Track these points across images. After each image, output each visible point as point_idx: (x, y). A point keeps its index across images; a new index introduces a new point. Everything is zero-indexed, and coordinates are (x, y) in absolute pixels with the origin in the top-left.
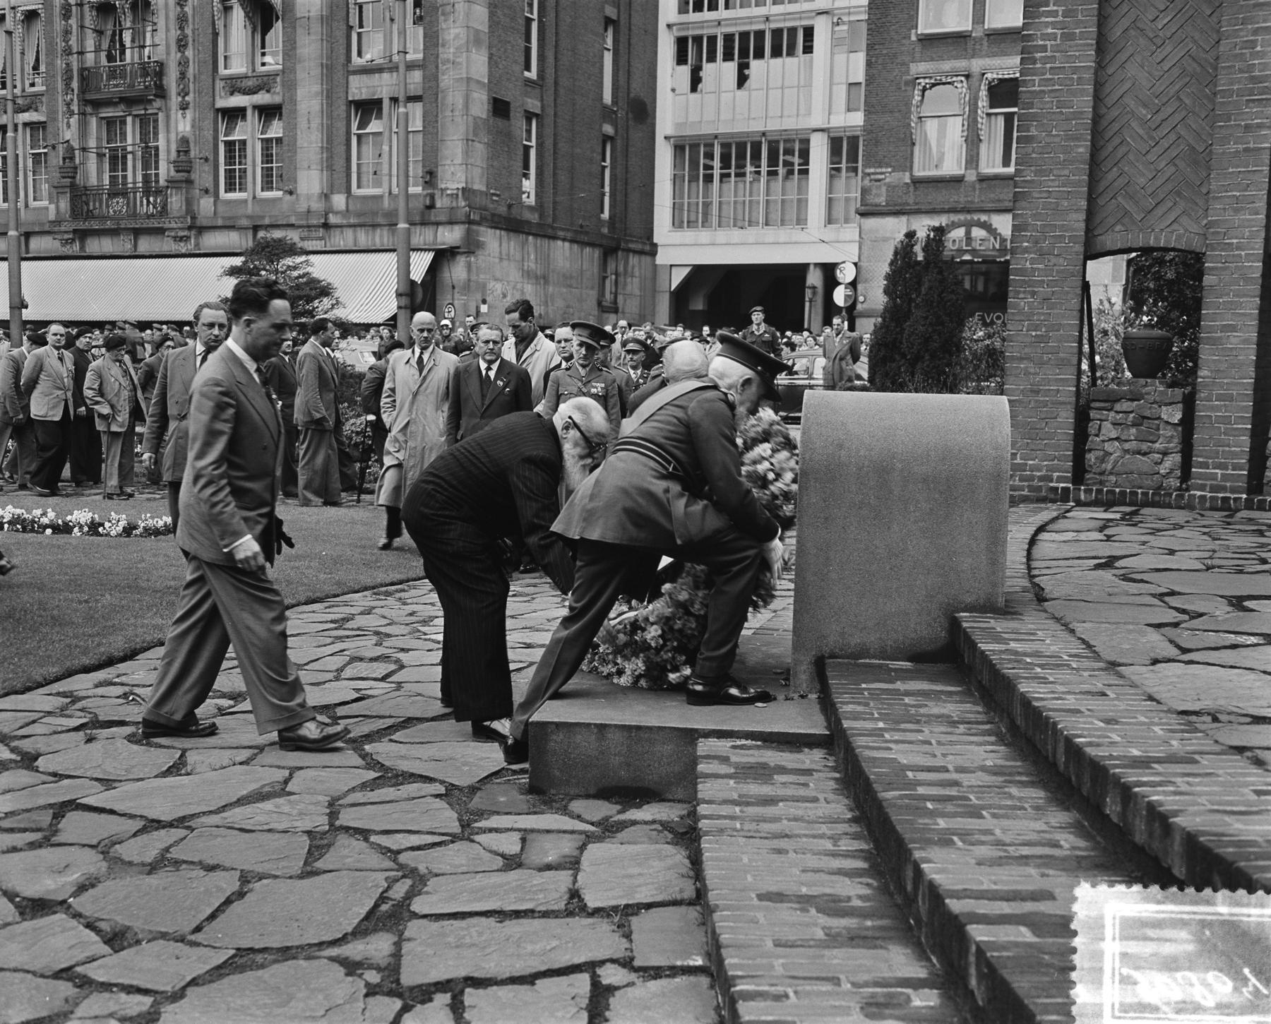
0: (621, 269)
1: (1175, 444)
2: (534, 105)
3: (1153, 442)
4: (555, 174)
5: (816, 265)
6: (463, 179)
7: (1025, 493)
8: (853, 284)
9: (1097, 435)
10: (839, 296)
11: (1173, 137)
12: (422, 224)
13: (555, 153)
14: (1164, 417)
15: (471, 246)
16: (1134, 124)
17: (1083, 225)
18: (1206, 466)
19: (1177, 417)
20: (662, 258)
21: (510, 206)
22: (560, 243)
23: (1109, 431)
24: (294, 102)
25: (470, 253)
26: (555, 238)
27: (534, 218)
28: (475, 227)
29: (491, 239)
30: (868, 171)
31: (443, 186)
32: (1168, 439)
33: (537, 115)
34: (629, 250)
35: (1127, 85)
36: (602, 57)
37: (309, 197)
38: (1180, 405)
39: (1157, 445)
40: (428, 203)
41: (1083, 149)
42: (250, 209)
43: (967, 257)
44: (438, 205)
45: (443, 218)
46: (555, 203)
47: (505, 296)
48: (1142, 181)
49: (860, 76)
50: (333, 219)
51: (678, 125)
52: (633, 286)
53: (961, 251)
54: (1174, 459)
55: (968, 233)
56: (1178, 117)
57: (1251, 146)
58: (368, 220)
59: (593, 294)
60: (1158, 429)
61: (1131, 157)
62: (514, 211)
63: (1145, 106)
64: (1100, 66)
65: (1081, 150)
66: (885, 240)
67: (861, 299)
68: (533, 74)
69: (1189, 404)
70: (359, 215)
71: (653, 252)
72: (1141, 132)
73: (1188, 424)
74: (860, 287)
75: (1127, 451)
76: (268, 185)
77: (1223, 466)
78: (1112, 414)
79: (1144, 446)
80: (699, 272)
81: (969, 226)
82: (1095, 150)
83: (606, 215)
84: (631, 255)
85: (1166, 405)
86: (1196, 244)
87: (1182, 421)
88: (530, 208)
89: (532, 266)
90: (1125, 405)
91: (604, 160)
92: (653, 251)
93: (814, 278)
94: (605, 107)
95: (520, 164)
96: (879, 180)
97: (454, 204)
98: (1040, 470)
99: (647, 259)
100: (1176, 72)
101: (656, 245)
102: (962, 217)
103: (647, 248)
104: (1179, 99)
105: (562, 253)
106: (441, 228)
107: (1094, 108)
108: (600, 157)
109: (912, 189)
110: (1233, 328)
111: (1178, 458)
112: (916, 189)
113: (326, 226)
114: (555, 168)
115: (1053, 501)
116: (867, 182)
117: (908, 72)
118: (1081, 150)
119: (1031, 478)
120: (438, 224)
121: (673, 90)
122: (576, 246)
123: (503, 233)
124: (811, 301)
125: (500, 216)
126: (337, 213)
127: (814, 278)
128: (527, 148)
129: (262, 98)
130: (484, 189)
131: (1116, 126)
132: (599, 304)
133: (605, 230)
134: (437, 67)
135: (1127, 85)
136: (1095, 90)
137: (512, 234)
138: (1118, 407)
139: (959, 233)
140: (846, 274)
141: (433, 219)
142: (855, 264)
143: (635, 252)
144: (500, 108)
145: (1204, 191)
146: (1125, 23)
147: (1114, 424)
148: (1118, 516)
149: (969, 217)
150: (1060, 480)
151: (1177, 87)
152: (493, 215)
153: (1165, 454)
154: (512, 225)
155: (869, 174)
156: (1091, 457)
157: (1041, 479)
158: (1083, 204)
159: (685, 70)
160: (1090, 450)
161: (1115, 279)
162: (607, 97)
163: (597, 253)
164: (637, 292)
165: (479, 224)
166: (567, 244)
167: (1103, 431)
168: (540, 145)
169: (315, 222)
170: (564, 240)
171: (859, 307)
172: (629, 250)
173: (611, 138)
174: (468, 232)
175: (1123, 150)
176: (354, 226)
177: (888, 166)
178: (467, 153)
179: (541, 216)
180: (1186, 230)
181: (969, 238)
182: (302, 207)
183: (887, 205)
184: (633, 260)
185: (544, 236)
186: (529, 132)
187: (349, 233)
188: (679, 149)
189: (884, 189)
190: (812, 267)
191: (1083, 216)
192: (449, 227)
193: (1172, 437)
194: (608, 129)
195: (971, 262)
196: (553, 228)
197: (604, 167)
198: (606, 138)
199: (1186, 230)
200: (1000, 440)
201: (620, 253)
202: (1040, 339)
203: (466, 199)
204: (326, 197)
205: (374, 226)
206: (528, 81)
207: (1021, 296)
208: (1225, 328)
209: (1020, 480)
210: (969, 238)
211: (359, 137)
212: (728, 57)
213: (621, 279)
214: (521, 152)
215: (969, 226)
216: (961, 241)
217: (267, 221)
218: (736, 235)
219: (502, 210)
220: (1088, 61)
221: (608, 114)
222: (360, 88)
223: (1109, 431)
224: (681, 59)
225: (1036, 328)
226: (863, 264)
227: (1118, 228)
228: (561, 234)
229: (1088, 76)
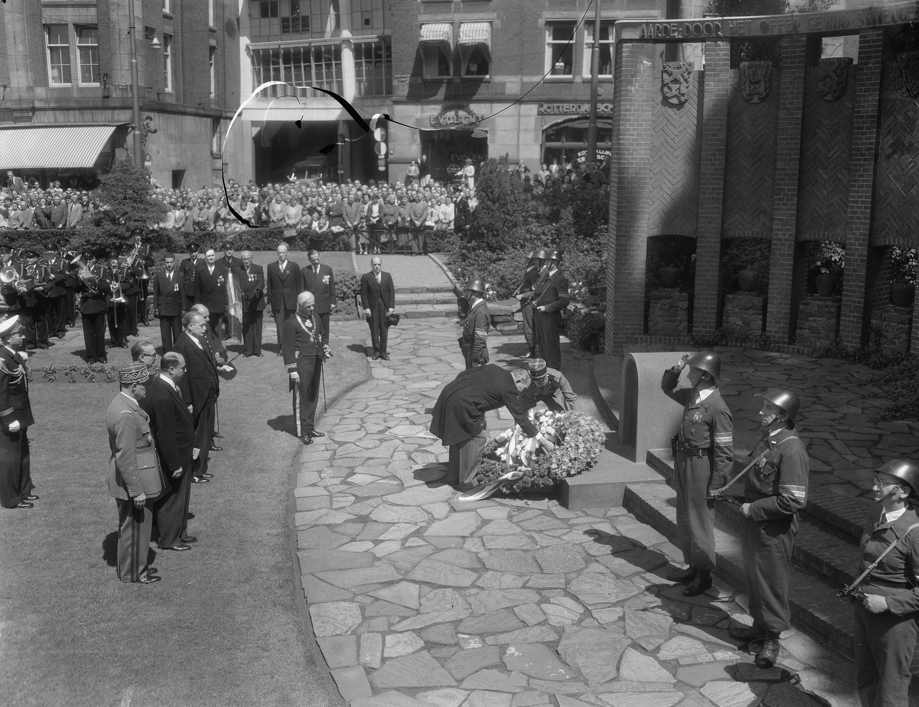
1: (685, 317)
18: (698, 327)
19: (686, 306)
32: (682, 316)
37: (19, 89)
45: (117, 104)
47: (158, 153)
54: (684, 324)
58: (64, 105)
67: (392, 152)
73: (690, 309)
77: (706, 327)
89: (173, 132)
134: (108, 7)
150: (640, 334)
156: (651, 324)
161: (536, 141)
171: (390, 157)
176: (54, 109)
182: (15, 96)
187: (50, 114)
204: (30, 89)
218: (293, 104)
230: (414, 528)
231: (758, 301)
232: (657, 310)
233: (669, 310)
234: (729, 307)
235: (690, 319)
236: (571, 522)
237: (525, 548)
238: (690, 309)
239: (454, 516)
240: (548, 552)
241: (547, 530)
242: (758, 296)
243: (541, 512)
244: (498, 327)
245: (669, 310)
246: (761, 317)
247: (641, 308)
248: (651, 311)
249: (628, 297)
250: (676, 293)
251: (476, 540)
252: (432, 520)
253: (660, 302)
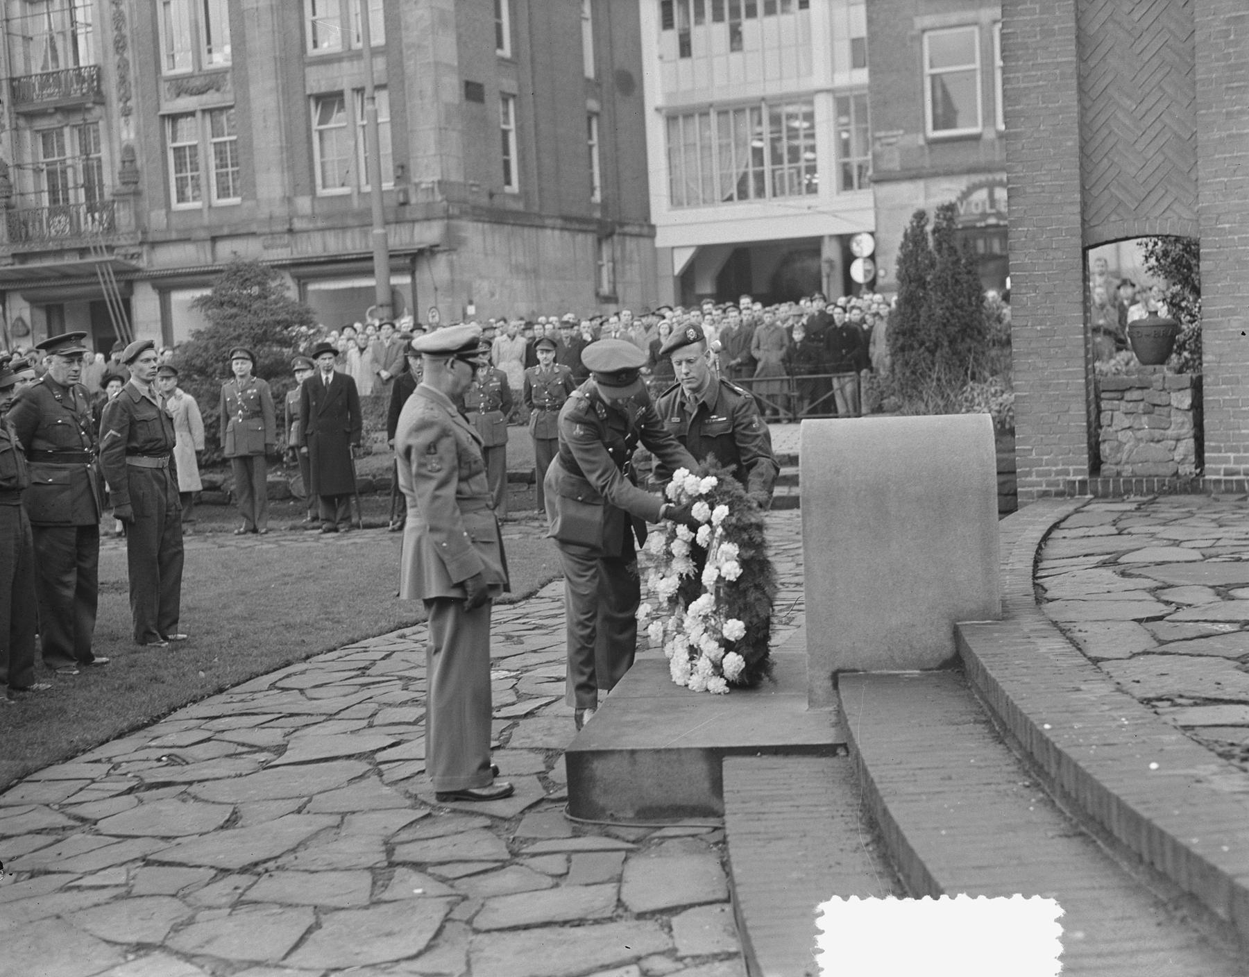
0: (618, 254)
2: (510, 85)
3: (1165, 429)
4: (538, 159)
5: (831, 236)
6: (438, 171)
7: (1044, 488)
8: (872, 257)
10: (858, 272)
11: (1158, 126)
12: (397, 223)
13: (536, 134)
15: (452, 243)
16: (1120, 115)
17: (1078, 218)
19: (1187, 402)
20: (660, 242)
21: (491, 195)
22: (549, 232)
23: (1121, 421)
24: (247, 100)
25: (451, 250)
26: (543, 227)
27: (519, 206)
28: (454, 222)
29: (474, 234)
30: (878, 134)
31: (417, 180)
32: (1182, 425)
33: (514, 96)
34: (625, 234)
35: (1110, 78)
36: (580, 28)
38: (1189, 392)
39: (1169, 432)
40: (401, 199)
41: (1072, 143)
42: (206, 220)
43: (992, 221)
44: (413, 200)
45: (419, 215)
46: (541, 190)
47: (493, 295)
48: (1133, 171)
49: (862, 32)
50: (298, 224)
51: (669, 95)
52: (633, 273)
53: (984, 216)
55: (991, 195)
56: (1161, 107)
57: (1234, 131)
59: (590, 285)
60: (1169, 416)
61: (1120, 146)
62: (497, 201)
63: (1129, 97)
64: (1082, 58)
65: (1070, 144)
66: (903, 207)
67: (881, 273)
68: (506, 52)
69: (1197, 387)
70: (328, 217)
71: (652, 236)
72: (1127, 122)
73: (1197, 407)
74: (879, 260)
75: (1139, 440)
76: (223, 192)
78: (1123, 403)
79: (1157, 434)
80: (704, 253)
81: (991, 186)
82: (1084, 145)
83: (597, 197)
84: (628, 238)
85: (1175, 391)
86: (1188, 231)
87: (1192, 406)
88: (513, 196)
89: (521, 259)
90: (1135, 395)
91: (590, 137)
92: (651, 231)
93: (831, 252)
94: (588, 80)
95: (499, 149)
96: (889, 144)
97: (430, 199)
98: (1056, 465)
99: (644, 242)
100: (1156, 62)
101: (653, 227)
102: (981, 178)
103: (645, 230)
104: (1161, 88)
105: (554, 244)
106: (417, 227)
107: (1080, 101)
108: (585, 136)
109: (927, 151)
110: (1232, 312)
111: (1189, 443)
112: (931, 151)
113: (290, 231)
114: (538, 151)
115: (1072, 495)
116: (878, 147)
117: (912, 26)
118: (1070, 144)
119: (1048, 473)
120: (414, 221)
121: (661, 57)
122: (566, 234)
123: (487, 226)
124: (828, 276)
125: (481, 208)
126: (303, 217)
127: (831, 252)
128: (505, 133)
129: (211, 99)
130: (461, 180)
131: (1102, 118)
132: (597, 294)
133: (597, 215)
134: (401, 52)
135: (1110, 78)
136: (1079, 84)
137: (496, 226)
138: (1128, 396)
139: (982, 195)
140: (863, 246)
141: (408, 216)
142: (872, 234)
143: (631, 235)
144: (473, 91)
145: (1194, 178)
146: (1103, 16)
148: (1134, 506)
149: (990, 177)
150: (1076, 472)
151: (1159, 76)
152: (474, 208)
153: (1178, 440)
154: (497, 216)
155: (880, 139)
157: (1058, 473)
158: (1078, 196)
159: (672, 36)
162: (590, 72)
163: (590, 239)
164: (638, 279)
165: (459, 217)
166: (557, 233)
167: (1115, 422)
168: (520, 128)
169: (279, 228)
170: (553, 228)
172: (625, 234)
173: (597, 114)
174: (448, 231)
175: (1111, 140)
176: (322, 230)
177: (898, 128)
178: (440, 143)
179: (526, 205)
180: (1180, 218)
181: (992, 201)
182: (263, 213)
183: (903, 169)
184: (631, 244)
185: (531, 226)
186: (506, 114)
187: (317, 238)
188: (672, 118)
189: (897, 154)
190: (826, 240)
191: (1077, 209)
192: (426, 224)
193: (1183, 423)
194: (593, 105)
195: (997, 226)
196: (541, 217)
197: (591, 147)
198: (590, 115)
199: (1180, 218)
200: (986, 457)
201: (615, 238)
203: (442, 192)
204: (289, 200)
205: (344, 228)
206: (502, 59)
207: (1024, 291)
210: (992, 201)
211: (321, 133)
212: (718, 18)
213: (619, 267)
214: (499, 136)
215: (991, 186)
216: (984, 203)
217: (226, 231)
219: (484, 201)
220: (1068, 56)
221: (593, 87)
222: (318, 81)
223: (1121, 421)
224: (667, 22)
226: (881, 235)
227: (1113, 218)
228: (548, 222)
229: (1071, 70)
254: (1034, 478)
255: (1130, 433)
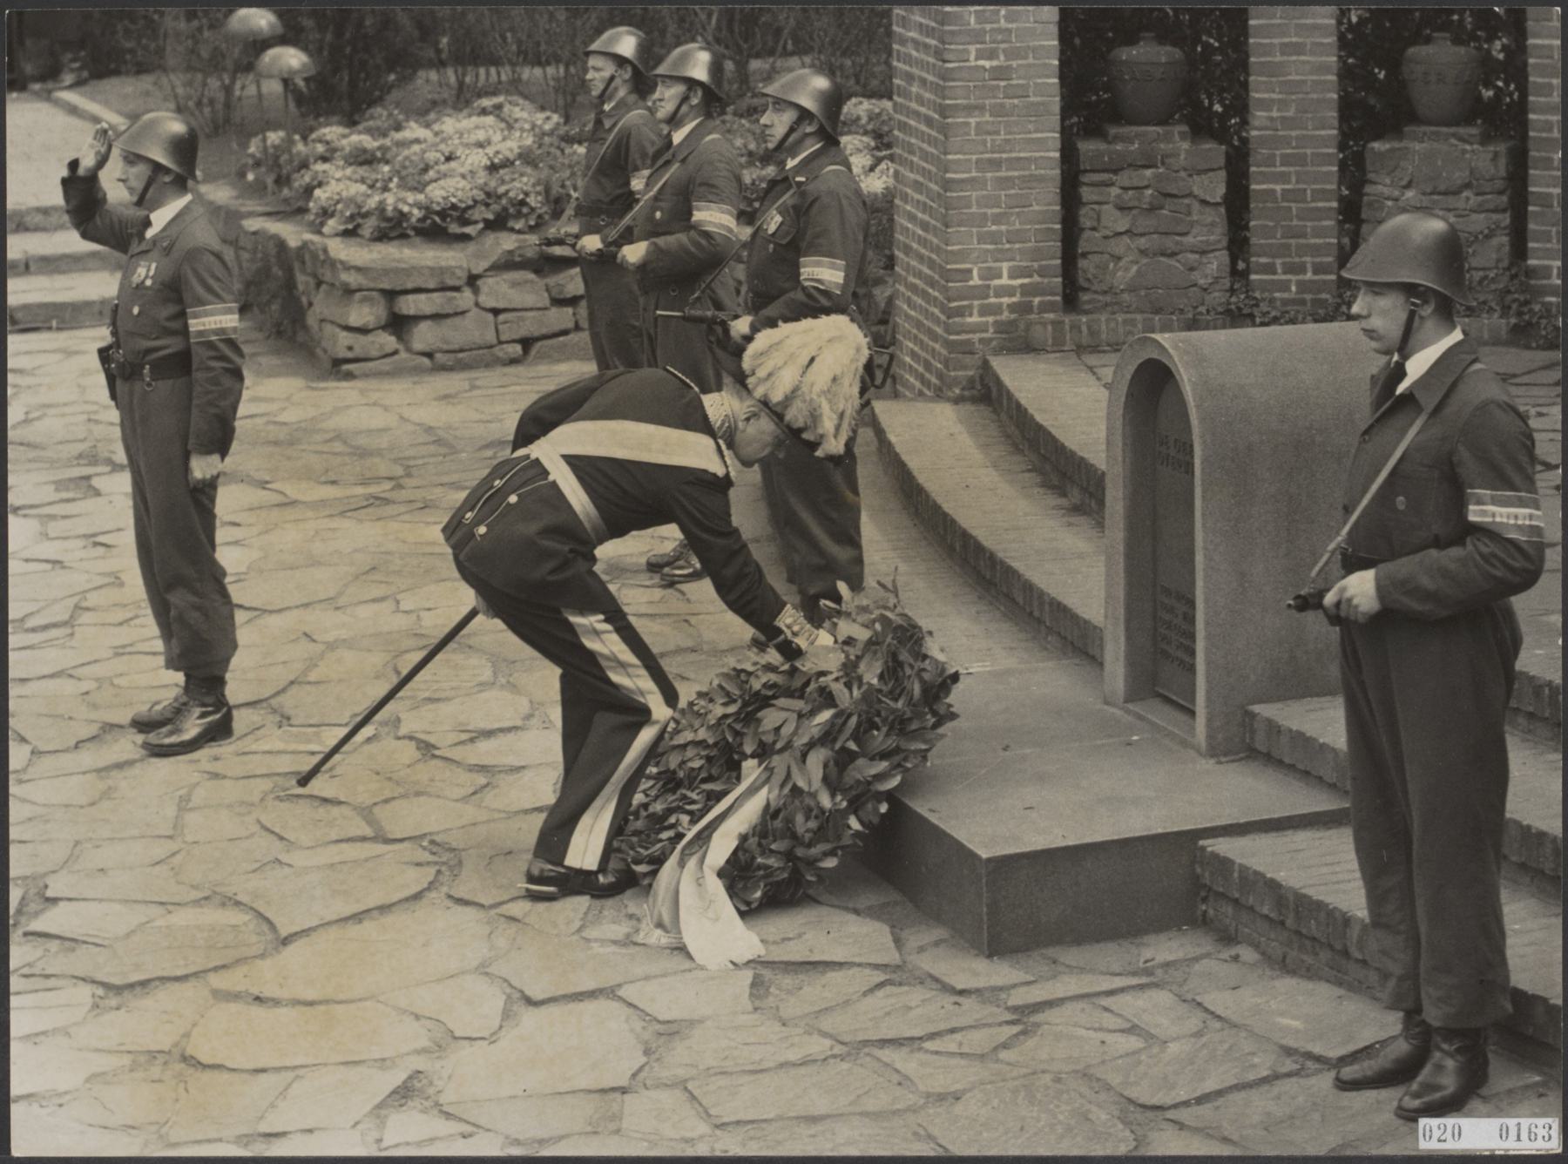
3: (1186, 234)
9: (1094, 229)
14: (1196, 191)
18: (1270, 269)
32: (1209, 229)
39: (1189, 240)
54: (1217, 263)
60: (1189, 214)
73: (1237, 203)
75: (1143, 252)
78: (1115, 191)
79: (1170, 243)
85: (1199, 172)
98: (1012, 295)
110: (1298, 49)
111: (1223, 257)
119: (995, 310)
147: (1121, 209)
160: (1084, 255)
167: (1104, 222)
193: (1213, 224)
202: (1000, 73)
208: (1287, 49)
209: (981, 314)
225: (991, 55)
230: (397, 1077)
231: (1487, 159)
232: (1105, 214)
233: (1153, 209)
234: (1380, 187)
235: (1238, 244)
236: (1019, 997)
237: (871, 1105)
238: (1237, 203)
239: (530, 1019)
240: (970, 1107)
241: (932, 1036)
242: (1485, 139)
243: (880, 977)
244: (424, 336)
245: (1153, 209)
246: (1505, 219)
247: (1046, 201)
248: (1085, 218)
249: (996, 164)
250: (1178, 144)
251: (668, 1098)
252: (446, 1040)
253: (1124, 178)
254: (975, 319)
255: (1126, 239)
